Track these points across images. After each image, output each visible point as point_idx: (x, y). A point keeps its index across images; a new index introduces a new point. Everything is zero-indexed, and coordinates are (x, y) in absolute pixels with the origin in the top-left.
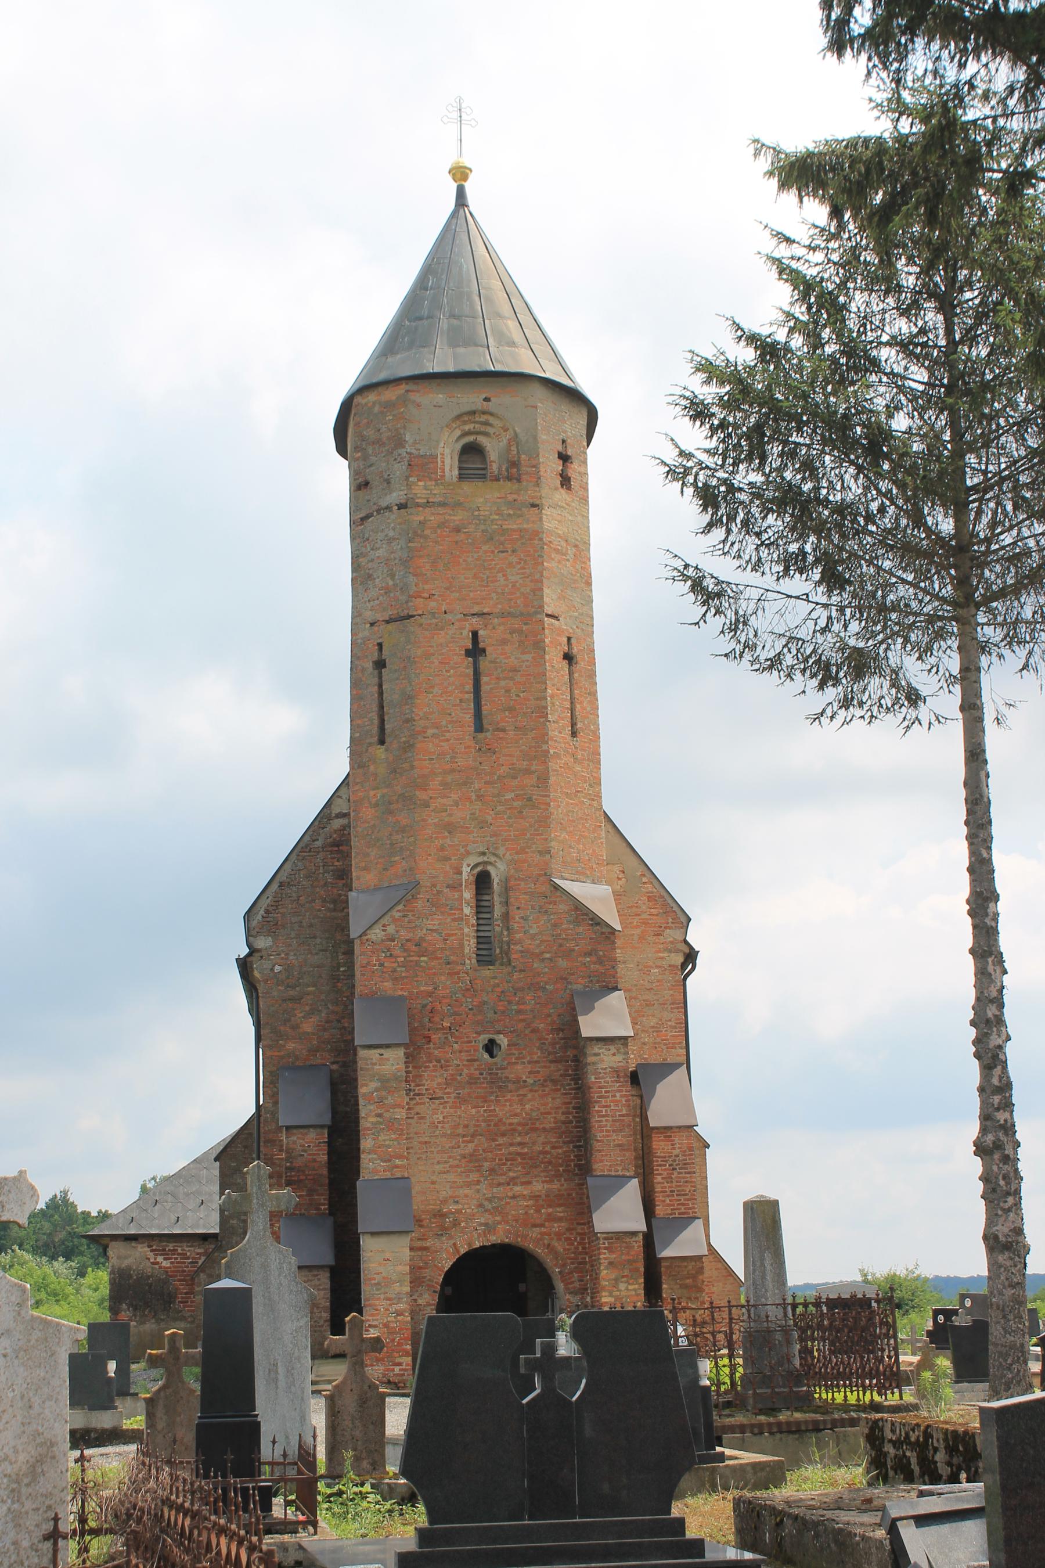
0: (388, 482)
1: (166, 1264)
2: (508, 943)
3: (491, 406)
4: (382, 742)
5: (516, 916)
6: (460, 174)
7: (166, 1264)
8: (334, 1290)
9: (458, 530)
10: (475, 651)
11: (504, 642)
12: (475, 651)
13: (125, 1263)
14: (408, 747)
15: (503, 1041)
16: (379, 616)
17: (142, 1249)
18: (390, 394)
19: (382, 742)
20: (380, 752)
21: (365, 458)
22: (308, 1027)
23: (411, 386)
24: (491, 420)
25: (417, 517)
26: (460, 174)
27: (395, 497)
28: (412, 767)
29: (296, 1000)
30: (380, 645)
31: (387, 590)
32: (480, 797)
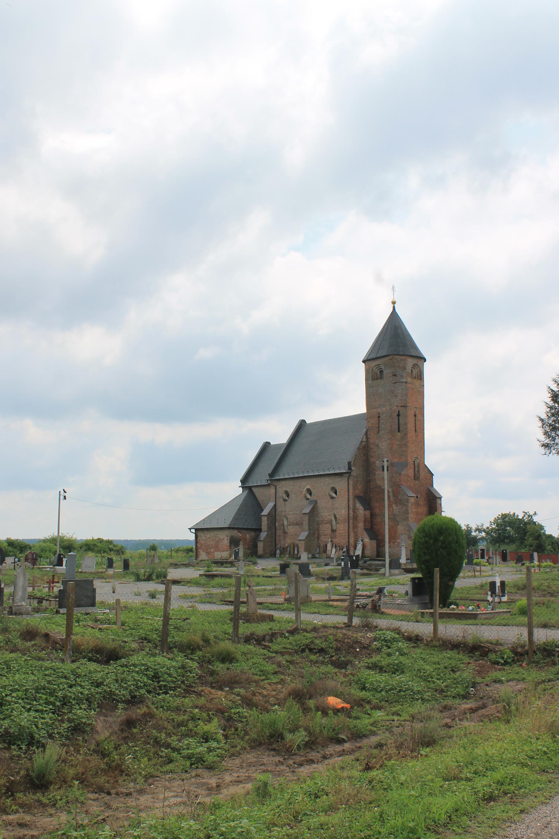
0: (402, 376)
1: (240, 535)
2: (419, 476)
3: (418, 363)
4: (399, 431)
5: (420, 471)
6: (394, 303)
7: (240, 535)
8: (377, 544)
9: (413, 389)
10: (415, 416)
11: (419, 414)
12: (415, 416)
13: (233, 534)
14: (406, 434)
15: (419, 496)
16: (399, 405)
17: (236, 531)
18: (403, 358)
19: (399, 431)
20: (399, 433)
21: (395, 369)
22: (360, 487)
23: (407, 357)
24: (417, 366)
25: (409, 385)
26: (394, 303)
27: (404, 380)
28: (407, 439)
29: (357, 481)
30: (399, 412)
31: (401, 400)
32: (416, 446)
